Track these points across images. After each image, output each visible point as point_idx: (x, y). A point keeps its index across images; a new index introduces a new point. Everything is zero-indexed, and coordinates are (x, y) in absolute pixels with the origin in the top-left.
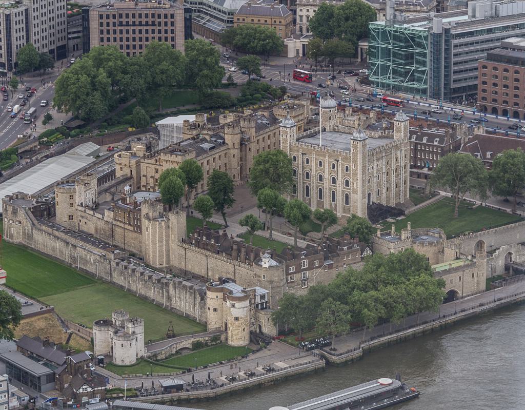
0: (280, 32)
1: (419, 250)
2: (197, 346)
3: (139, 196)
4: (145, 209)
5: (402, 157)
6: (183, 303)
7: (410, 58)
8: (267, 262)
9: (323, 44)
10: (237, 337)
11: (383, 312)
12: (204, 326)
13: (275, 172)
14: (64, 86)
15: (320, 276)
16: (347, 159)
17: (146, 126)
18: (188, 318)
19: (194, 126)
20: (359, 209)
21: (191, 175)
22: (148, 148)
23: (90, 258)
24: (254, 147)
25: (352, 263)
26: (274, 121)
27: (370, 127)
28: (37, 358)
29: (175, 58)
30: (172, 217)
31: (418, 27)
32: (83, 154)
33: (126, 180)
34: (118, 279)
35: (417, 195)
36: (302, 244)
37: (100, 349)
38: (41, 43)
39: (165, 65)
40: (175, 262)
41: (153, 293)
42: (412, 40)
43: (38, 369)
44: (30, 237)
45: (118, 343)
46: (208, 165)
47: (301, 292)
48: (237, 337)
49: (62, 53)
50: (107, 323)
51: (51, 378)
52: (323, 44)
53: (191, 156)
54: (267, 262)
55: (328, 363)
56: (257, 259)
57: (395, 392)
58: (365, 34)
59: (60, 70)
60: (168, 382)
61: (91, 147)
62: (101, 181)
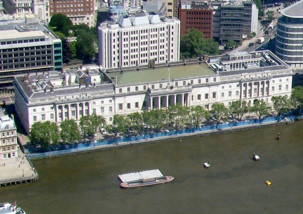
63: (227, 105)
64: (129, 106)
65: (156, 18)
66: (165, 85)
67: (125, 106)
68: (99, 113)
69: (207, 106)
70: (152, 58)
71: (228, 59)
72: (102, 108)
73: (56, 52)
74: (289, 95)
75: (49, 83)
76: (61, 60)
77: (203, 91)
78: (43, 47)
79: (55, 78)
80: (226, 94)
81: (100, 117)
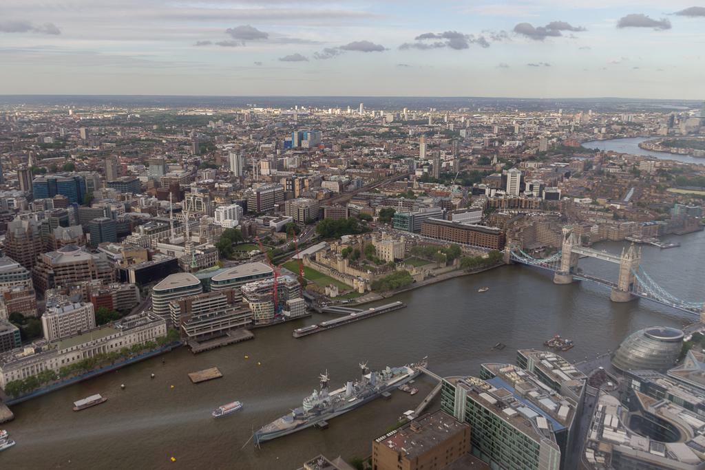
0: (372, 215)
1: (407, 270)
2: (351, 293)
3: (337, 255)
4: (338, 258)
5: (403, 247)
6: (348, 282)
7: (404, 222)
8: (369, 272)
9: (383, 218)
10: (361, 291)
11: (398, 285)
12: (353, 288)
13: (371, 249)
14: (318, 227)
15: (382, 276)
16: (387, 247)
17: (339, 238)
18: (349, 286)
19: (350, 238)
20: (391, 259)
21: (350, 250)
22: (339, 243)
23: (325, 271)
24: (365, 244)
25: (390, 273)
26: (370, 237)
27: (394, 239)
28: (311, 295)
29: (345, 221)
30: (345, 261)
31: (406, 215)
32: (322, 245)
33: (333, 251)
34: (331, 276)
35: (406, 256)
36: (377, 268)
37: (327, 293)
38: (312, 217)
39: (343, 223)
40: (346, 272)
41: (340, 279)
42: (404, 218)
43: (311, 298)
44: (309, 265)
45: (331, 291)
46: (354, 248)
47: (377, 280)
48: (361, 291)
49: (317, 219)
50: (329, 286)
51: (315, 300)
52: (383, 218)
53: (350, 245)
54: (369, 272)
55: (384, 298)
56: (366, 271)
57: (400, 305)
58: (393, 216)
59: (316, 223)
60: (344, 302)
61: (325, 243)
62: (327, 251)
63: (129, 348)
64: (68, 360)
65: (77, 305)
66: (89, 343)
67: (66, 361)
68: (49, 368)
69: (117, 351)
70: (79, 329)
71: (126, 321)
72: (51, 365)
73: (16, 336)
74: (166, 335)
75: (14, 356)
76: (20, 341)
77: (113, 342)
78: (7, 335)
79: (18, 352)
80: (128, 342)
81: (51, 371)
